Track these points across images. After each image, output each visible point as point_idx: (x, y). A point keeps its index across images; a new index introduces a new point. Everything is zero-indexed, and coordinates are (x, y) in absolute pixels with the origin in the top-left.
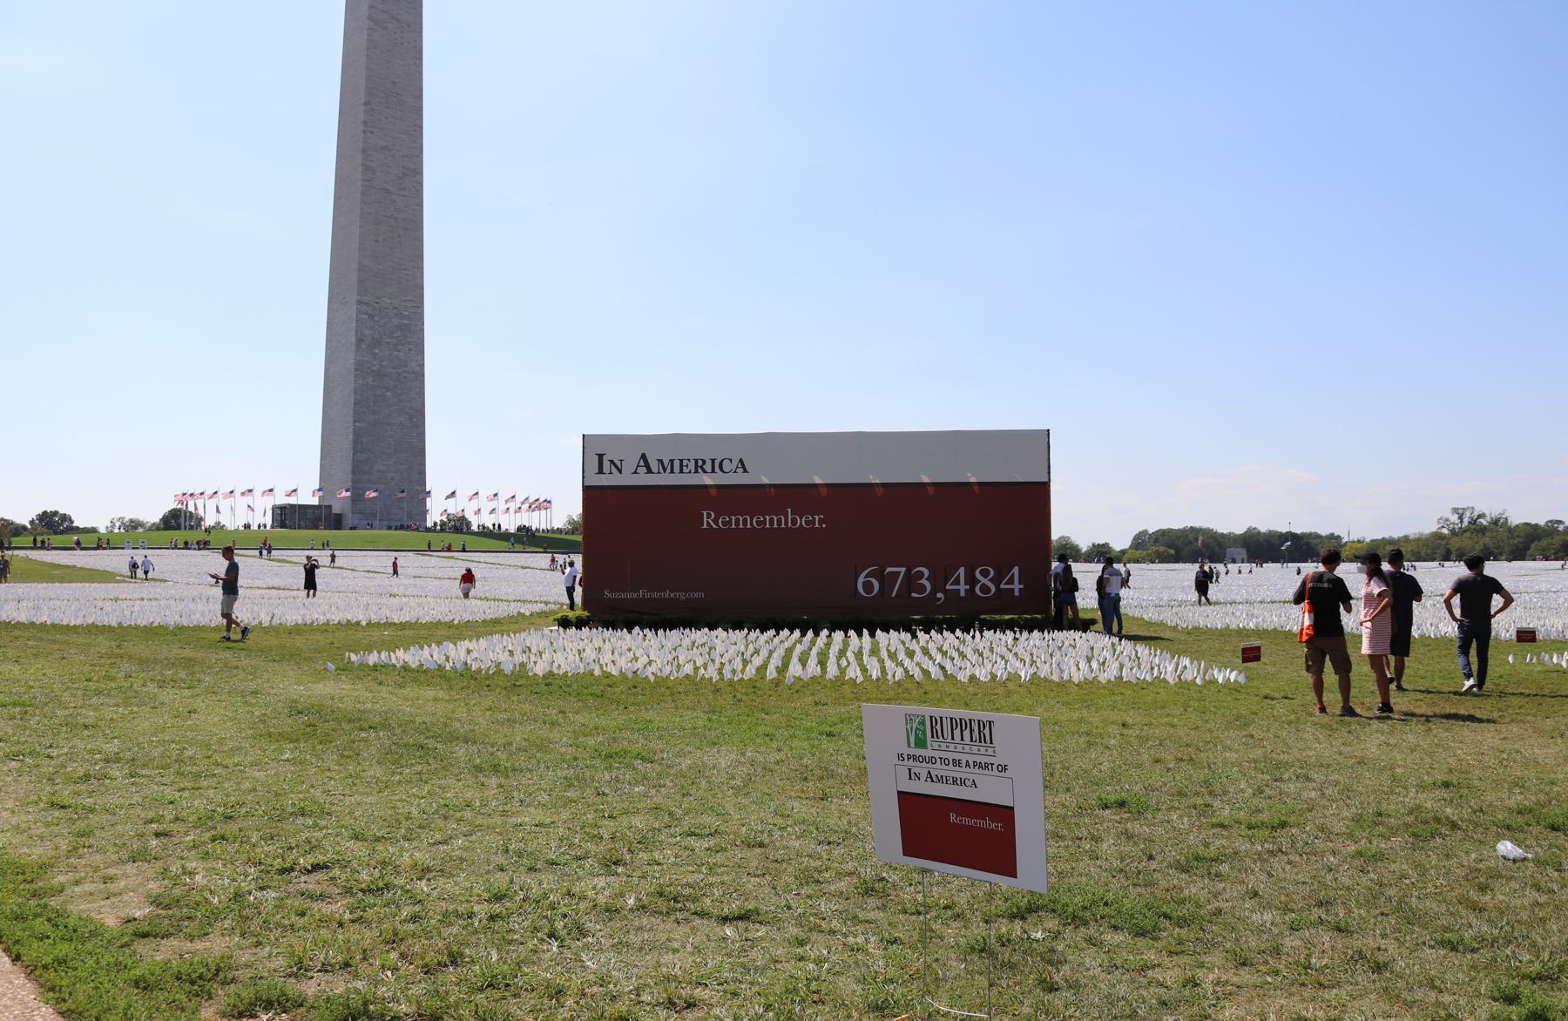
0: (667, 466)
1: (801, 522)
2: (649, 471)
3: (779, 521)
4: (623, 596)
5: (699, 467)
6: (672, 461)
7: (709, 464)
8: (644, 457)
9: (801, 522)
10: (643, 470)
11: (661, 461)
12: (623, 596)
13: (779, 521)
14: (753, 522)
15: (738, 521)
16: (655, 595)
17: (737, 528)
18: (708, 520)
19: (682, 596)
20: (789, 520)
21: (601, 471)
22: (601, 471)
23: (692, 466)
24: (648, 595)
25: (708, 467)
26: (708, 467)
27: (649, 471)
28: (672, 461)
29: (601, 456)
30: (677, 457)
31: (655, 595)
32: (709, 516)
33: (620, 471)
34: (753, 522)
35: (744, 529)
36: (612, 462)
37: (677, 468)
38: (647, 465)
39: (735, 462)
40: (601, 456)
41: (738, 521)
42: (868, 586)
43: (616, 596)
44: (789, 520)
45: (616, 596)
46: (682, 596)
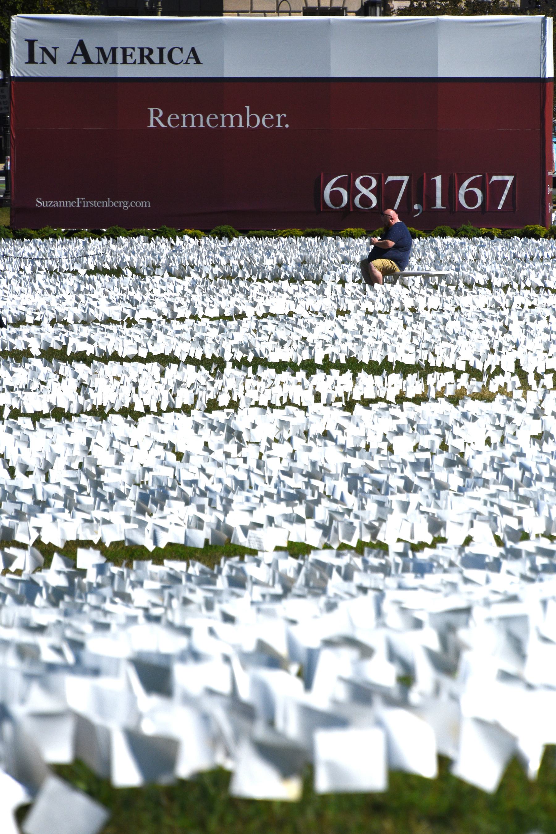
0: (108, 56)
1: (261, 121)
2: (88, 61)
3: (236, 120)
4: (58, 204)
5: (145, 56)
7: (156, 53)
8: (81, 44)
9: (261, 121)
11: (101, 50)
12: (58, 204)
13: (236, 120)
14: (206, 121)
15: (191, 120)
16: (95, 204)
17: (189, 129)
18: (155, 118)
19: (125, 205)
20: (248, 119)
21: (31, 60)
22: (31, 60)
23: (137, 55)
24: (86, 204)
25: (155, 57)
26: (155, 57)
27: (88, 61)
28: (114, 50)
29: (31, 43)
30: (120, 45)
31: (95, 204)
32: (156, 113)
33: (54, 60)
34: (206, 121)
35: (197, 129)
36: (44, 50)
38: (85, 54)
39: (187, 50)
40: (31, 43)
41: (191, 120)
42: (336, 197)
43: (49, 204)
44: (248, 119)
45: (49, 204)
46: (125, 205)
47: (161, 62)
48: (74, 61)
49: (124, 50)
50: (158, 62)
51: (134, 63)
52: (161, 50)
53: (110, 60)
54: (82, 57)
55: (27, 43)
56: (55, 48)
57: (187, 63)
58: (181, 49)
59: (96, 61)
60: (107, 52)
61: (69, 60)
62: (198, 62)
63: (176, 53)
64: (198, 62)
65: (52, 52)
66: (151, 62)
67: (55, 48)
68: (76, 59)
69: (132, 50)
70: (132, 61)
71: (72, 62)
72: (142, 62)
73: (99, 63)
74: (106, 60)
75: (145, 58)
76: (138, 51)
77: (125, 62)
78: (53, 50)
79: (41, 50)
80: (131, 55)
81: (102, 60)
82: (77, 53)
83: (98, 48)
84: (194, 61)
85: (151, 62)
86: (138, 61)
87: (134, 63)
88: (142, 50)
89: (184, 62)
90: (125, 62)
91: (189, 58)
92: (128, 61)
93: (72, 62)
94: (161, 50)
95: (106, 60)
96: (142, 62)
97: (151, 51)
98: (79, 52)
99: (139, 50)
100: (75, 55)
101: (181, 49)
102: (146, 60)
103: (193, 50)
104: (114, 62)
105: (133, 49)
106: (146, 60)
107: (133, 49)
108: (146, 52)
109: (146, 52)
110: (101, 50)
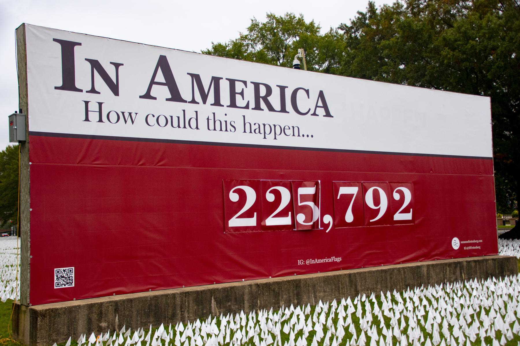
6: (216, 81)
8: (163, 63)
10: (162, 92)
11: (196, 78)
22: (69, 83)
25: (275, 100)
26: (275, 100)
33: (115, 89)
36: (95, 65)
37: (225, 98)
38: (170, 82)
47: (283, 110)
48: (152, 94)
49: (232, 82)
50: (279, 110)
51: (247, 107)
52: (282, 89)
53: (211, 99)
54: (166, 88)
55: (59, 46)
56: (117, 66)
57: (314, 114)
58: (307, 91)
59: (190, 99)
60: (206, 83)
61: (144, 93)
62: (328, 114)
63: (301, 94)
64: (328, 114)
65: (111, 71)
66: (271, 108)
67: (117, 66)
68: (155, 90)
69: (243, 86)
70: (244, 105)
71: (147, 96)
72: (258, 107)
73: (193, 101)
74: (204, 98)
75: (261, 99)
76: (251, 88)
77: (233, 104)
78: (113, 67)
79: (89, 65)
80: (242, 94)
81: (198, 97)
82: (155, 80)
83: (192, 75)
84: (321, 112)
85: (271, 108)
86: (252, 105)
87: (247, 107)
88: (257, 86)
89: (312, 112)
90: (233, 104)
91: (317, 106)
92: (238, 104)
93: (147, 96)
94: (282, 89)
95: (204, 98)
96: (258, 107)
97: (269, 91)
98: (160, 77)
99: (253, 85)
100: (153, 82)
101: (307, 91)
102: (263, 105)
103: (321, 95)
104: (217, 103)
105: (245, 83)
106: (263, 105)
107: (245, 83)
108: (263, 92)
109: (263, 92)
110: (196, 78)
